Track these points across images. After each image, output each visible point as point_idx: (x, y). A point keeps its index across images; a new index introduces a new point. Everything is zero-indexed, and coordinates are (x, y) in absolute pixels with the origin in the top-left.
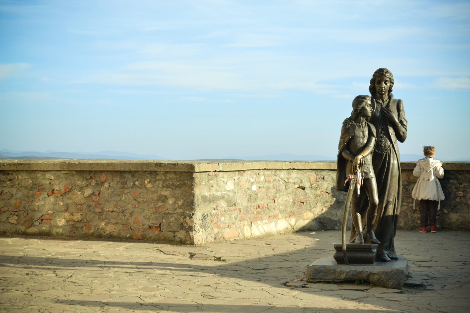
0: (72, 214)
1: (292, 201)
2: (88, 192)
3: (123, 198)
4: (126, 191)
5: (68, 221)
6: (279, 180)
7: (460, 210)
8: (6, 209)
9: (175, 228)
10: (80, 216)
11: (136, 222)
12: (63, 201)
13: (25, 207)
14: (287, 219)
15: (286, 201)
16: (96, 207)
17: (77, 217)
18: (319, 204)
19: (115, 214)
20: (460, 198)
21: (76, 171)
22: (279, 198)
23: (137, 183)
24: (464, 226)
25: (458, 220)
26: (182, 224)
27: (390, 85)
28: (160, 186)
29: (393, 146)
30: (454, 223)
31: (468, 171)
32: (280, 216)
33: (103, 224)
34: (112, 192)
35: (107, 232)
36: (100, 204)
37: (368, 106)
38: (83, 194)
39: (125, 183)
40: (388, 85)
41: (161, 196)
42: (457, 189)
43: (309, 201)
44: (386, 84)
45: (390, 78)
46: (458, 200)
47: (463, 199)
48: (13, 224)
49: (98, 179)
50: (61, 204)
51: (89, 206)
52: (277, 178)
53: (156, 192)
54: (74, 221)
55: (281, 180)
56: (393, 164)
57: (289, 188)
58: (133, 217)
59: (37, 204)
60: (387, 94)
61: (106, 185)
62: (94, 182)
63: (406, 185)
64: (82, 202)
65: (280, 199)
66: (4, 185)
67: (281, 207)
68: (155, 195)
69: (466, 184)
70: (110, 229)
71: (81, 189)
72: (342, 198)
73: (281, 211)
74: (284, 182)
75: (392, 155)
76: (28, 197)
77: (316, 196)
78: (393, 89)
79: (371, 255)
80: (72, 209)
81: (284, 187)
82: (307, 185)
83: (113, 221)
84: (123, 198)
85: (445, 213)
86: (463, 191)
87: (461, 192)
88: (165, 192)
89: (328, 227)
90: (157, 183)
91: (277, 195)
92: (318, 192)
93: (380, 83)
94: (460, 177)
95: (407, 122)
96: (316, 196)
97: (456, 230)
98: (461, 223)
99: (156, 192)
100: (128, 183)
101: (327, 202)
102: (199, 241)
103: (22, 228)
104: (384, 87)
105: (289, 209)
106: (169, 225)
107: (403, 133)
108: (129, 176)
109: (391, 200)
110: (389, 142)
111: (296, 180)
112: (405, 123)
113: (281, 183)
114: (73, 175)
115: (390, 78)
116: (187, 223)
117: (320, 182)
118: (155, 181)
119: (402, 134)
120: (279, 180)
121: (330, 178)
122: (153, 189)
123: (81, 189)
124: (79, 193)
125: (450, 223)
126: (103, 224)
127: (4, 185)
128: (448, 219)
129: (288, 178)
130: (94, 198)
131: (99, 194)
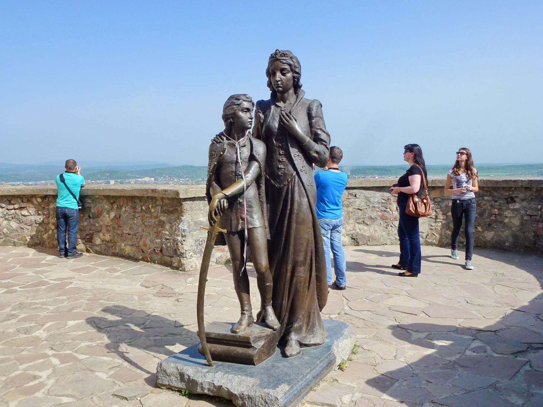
0: (104, 235)
2: (112, 215)
3: (135, 222)
4: (137, 215)
5: (103, 241)
7: (495, 228)
9: (171, 253)
10: (109, 237)
11: (145, 245)
16: (118, 229)
17: (108, 237)
18: (351, 221)
19: (130, 236)
20: (495, 217)
23: (144, 208)
24: (499, 246)
25: (493, 238)
26: (176, 250)
27: (294, 77)
28: (160, 212)
29: (298, 174)
30: (489, 241)
31: (504, 187)
33: (123, 244)
34: (127, 216)
35: (126, 253)
36: (120, 227)
37: (242, 111)
38: (109, 217)
39: (135, 208)
40: (289, 75)
41: (160, 221)
42: (492, 206)
44: (284, 74)
45: (290, 65)
46: (493, 218)
47: (498, 217)
49: (118, 203)
51: (114, 228)
53: (156, 217)
54: (106, 241)
56: (300, 204)
58: (143, 239)
60: (291, 91)
61: (124, 209)
62: (115, 206)
63: (440, 202)
64: (110, 223)
68: (157, 220)
69: (501, 202)
70: (128, 250)
71: (108, 213)
75: (296, 189)
77: (348, 213)
78: (302, 81)
79: (250, 351)
80: (104, 230)
83: (130, 243)
84: (135, 222)
85: (479, 231)
86: (498, 209)
87: (496, 210)
88: (163, 218)
89: (360, 243)
90: (157, 208)
92: (350, 209)
93: (274, 74)
94: (496, 194)
95: (328, 135)
96: (348, 213)
97: (490, 248)
98: (496, 242)
99: (156, 217)
100: (137, 208)
101: (359, 219)
102: (192, 267)
104: (281, 80)
106: (167, 250)
107: (317, 152)
108: (137, 201)
109: (301, 258)
110: (290, 168)
112: (323, 136)
114: (102, 199)
115: (290, 65)
116: (179, 249)
117: (352, 200)
118: (155, 207)
119: (316, 155)
121: (362, 196)
122: (155, 214)
123: (108, 213)
124: (107, 216)
125: (485, 242)
126: (123, 244)
128: (483, 237)
131: (120, 217)
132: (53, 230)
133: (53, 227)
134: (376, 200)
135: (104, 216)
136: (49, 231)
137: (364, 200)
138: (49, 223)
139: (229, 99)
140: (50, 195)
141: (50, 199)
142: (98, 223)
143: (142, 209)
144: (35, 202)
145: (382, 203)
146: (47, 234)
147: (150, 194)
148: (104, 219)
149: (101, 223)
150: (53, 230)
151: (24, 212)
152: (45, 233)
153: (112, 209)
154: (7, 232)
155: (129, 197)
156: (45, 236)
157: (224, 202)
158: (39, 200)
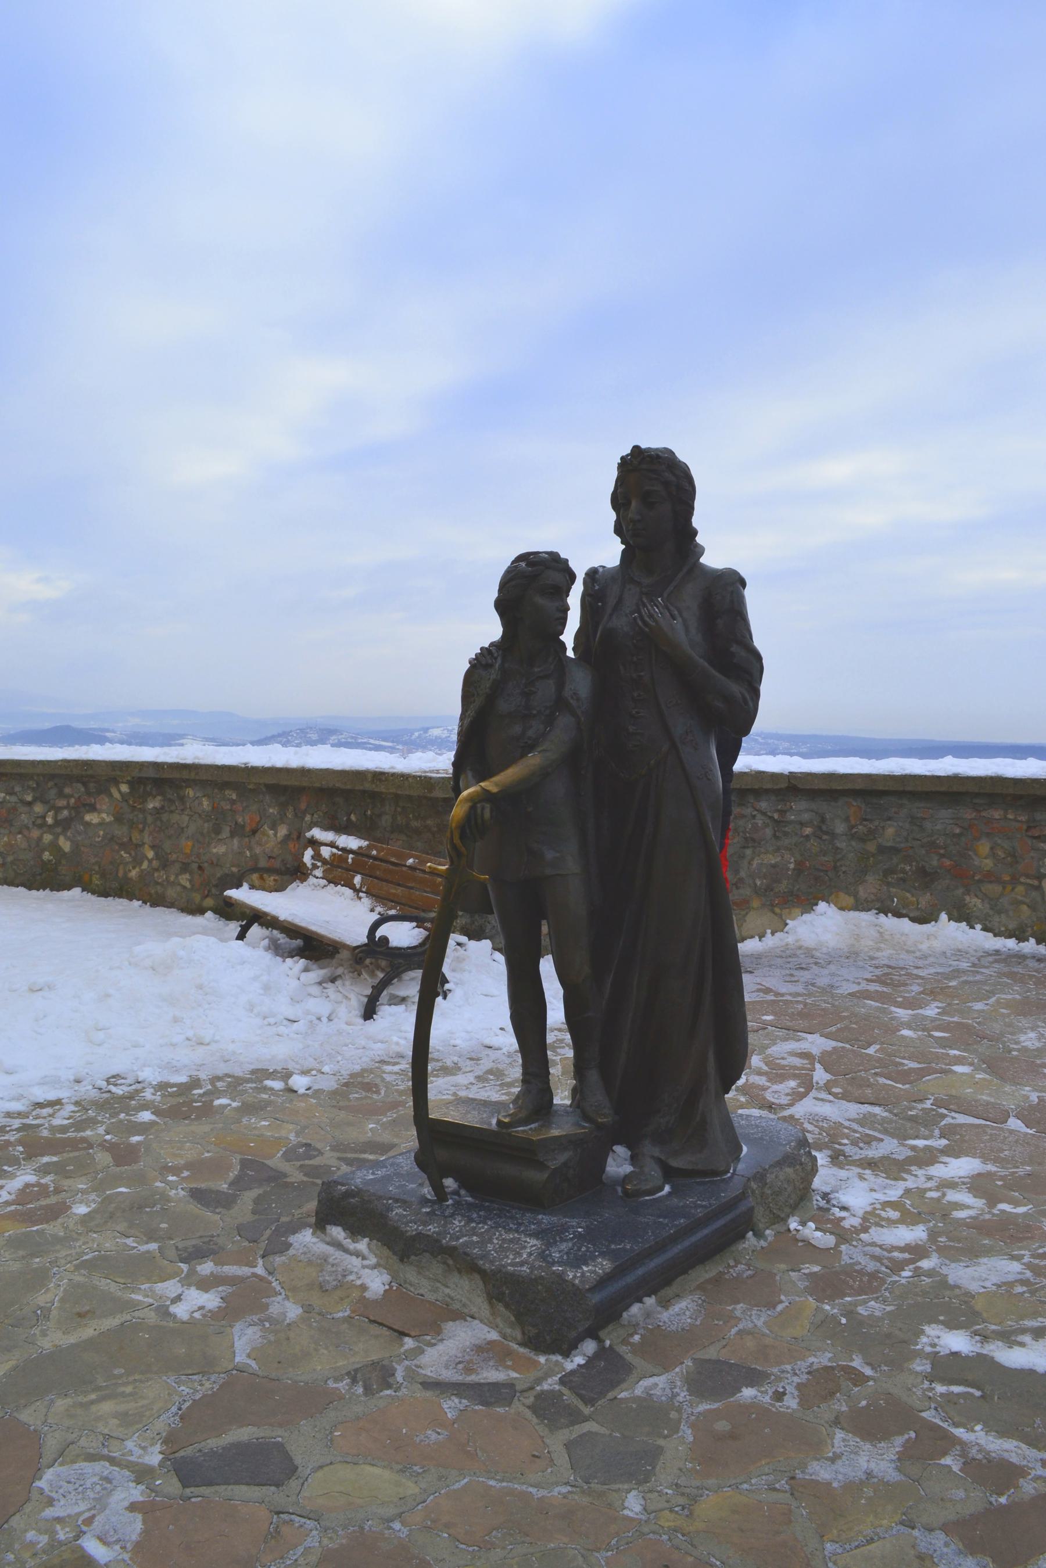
1: (792, 866)
2: (283, 831)
6: (754, 817)
8: (174, 856)
12: (250, 849)
13: (198, 856)
14: (777, 910)
15: (774, 866)
21: (267, 786)
22: (753, 859)
23: (353, 817)
32: (755, 903)
38: (275, 835)
43: (844, 869)
48: (184, 887)
50: (248, 853)
52: (748, 811)
55: (759, 816)
57: (786, 834)
59: (215, 851)
65: (755, 862)
66: (173, 808)
67: (758, 883)
71: (274, 827)
72: (935, 863)
73: (756, 890)
74: (768, 821)
76: (202, 834)
81: (769, 832)
82: (840, 828)
91: (748, 852)
92: (871, 847)
103: (197, 897)
105: (783, 886)
111: (806, 817)
113: (760, 823)
117: (876, 823)
120: (754, 817)
123: (274, 827)
127: (173, 808)
129: (782, 812)
130: (291, 845)
132: (150, 861)
133: (151, 854)
134: (938, 827)
135: (264, 834)
136: (141, 864)
137: (907, 826)
138: (144, 844)
139: (513, 562)
140: (147, 779)
141: (148, 789)
142: (250, 849)
143: (349, 819)
144: (116, 795)
145: (955, 835)
146: (137, 869)
147: (368, 786)
148: (264, 839)
149: (258, 850)
150: (150, 861)
151: (91, 818)
152: (134, 868)
153: (282, 818)
154: (50, 861)
155: (321, 790)
156: (134, 873)
157: (483, 808)
158: (124, 788)
